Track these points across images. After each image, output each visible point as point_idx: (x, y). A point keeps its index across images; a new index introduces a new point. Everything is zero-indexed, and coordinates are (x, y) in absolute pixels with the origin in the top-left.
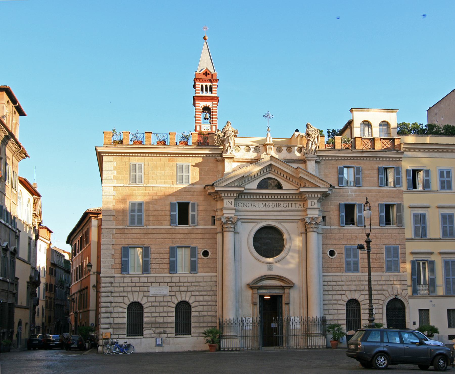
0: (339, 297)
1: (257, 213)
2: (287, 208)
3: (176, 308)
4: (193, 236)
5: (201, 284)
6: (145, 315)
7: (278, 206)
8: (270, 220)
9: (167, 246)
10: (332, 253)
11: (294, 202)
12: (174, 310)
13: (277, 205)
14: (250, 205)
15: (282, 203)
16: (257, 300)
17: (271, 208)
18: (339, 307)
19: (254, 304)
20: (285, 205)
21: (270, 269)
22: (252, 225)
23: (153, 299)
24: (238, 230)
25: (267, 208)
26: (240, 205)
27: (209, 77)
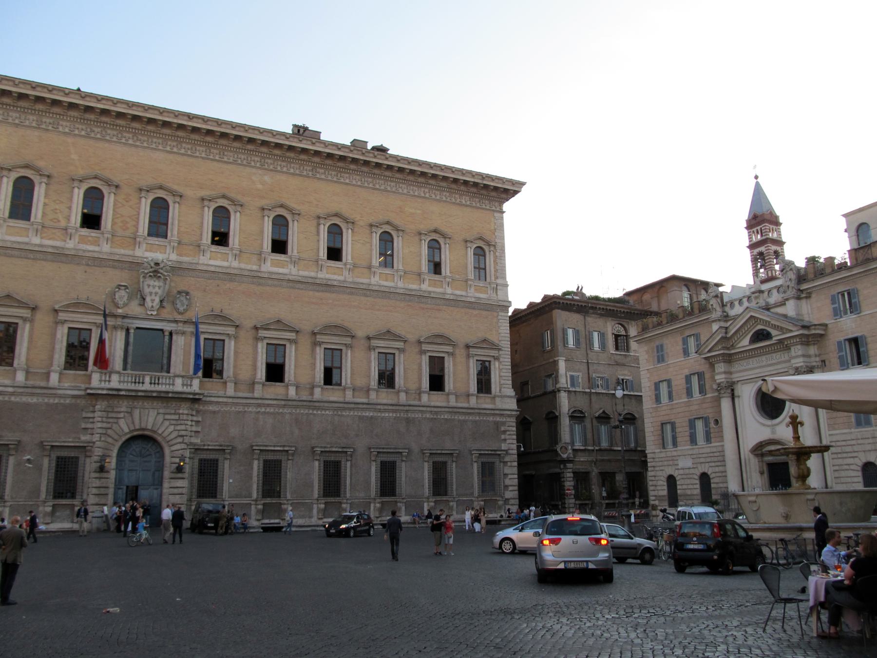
0: (851, 461)
1: (750, 372)
4: (704, 405)
5: (715, 454)
6: (678, 487)
9: (687, 419)
12: (698, 482)
15: (774, 355)
16: (765, 469)
17: (764, 363)
19: (762, 473)
21: (773, 432)
23: (681, 472)
27: (758, 220)
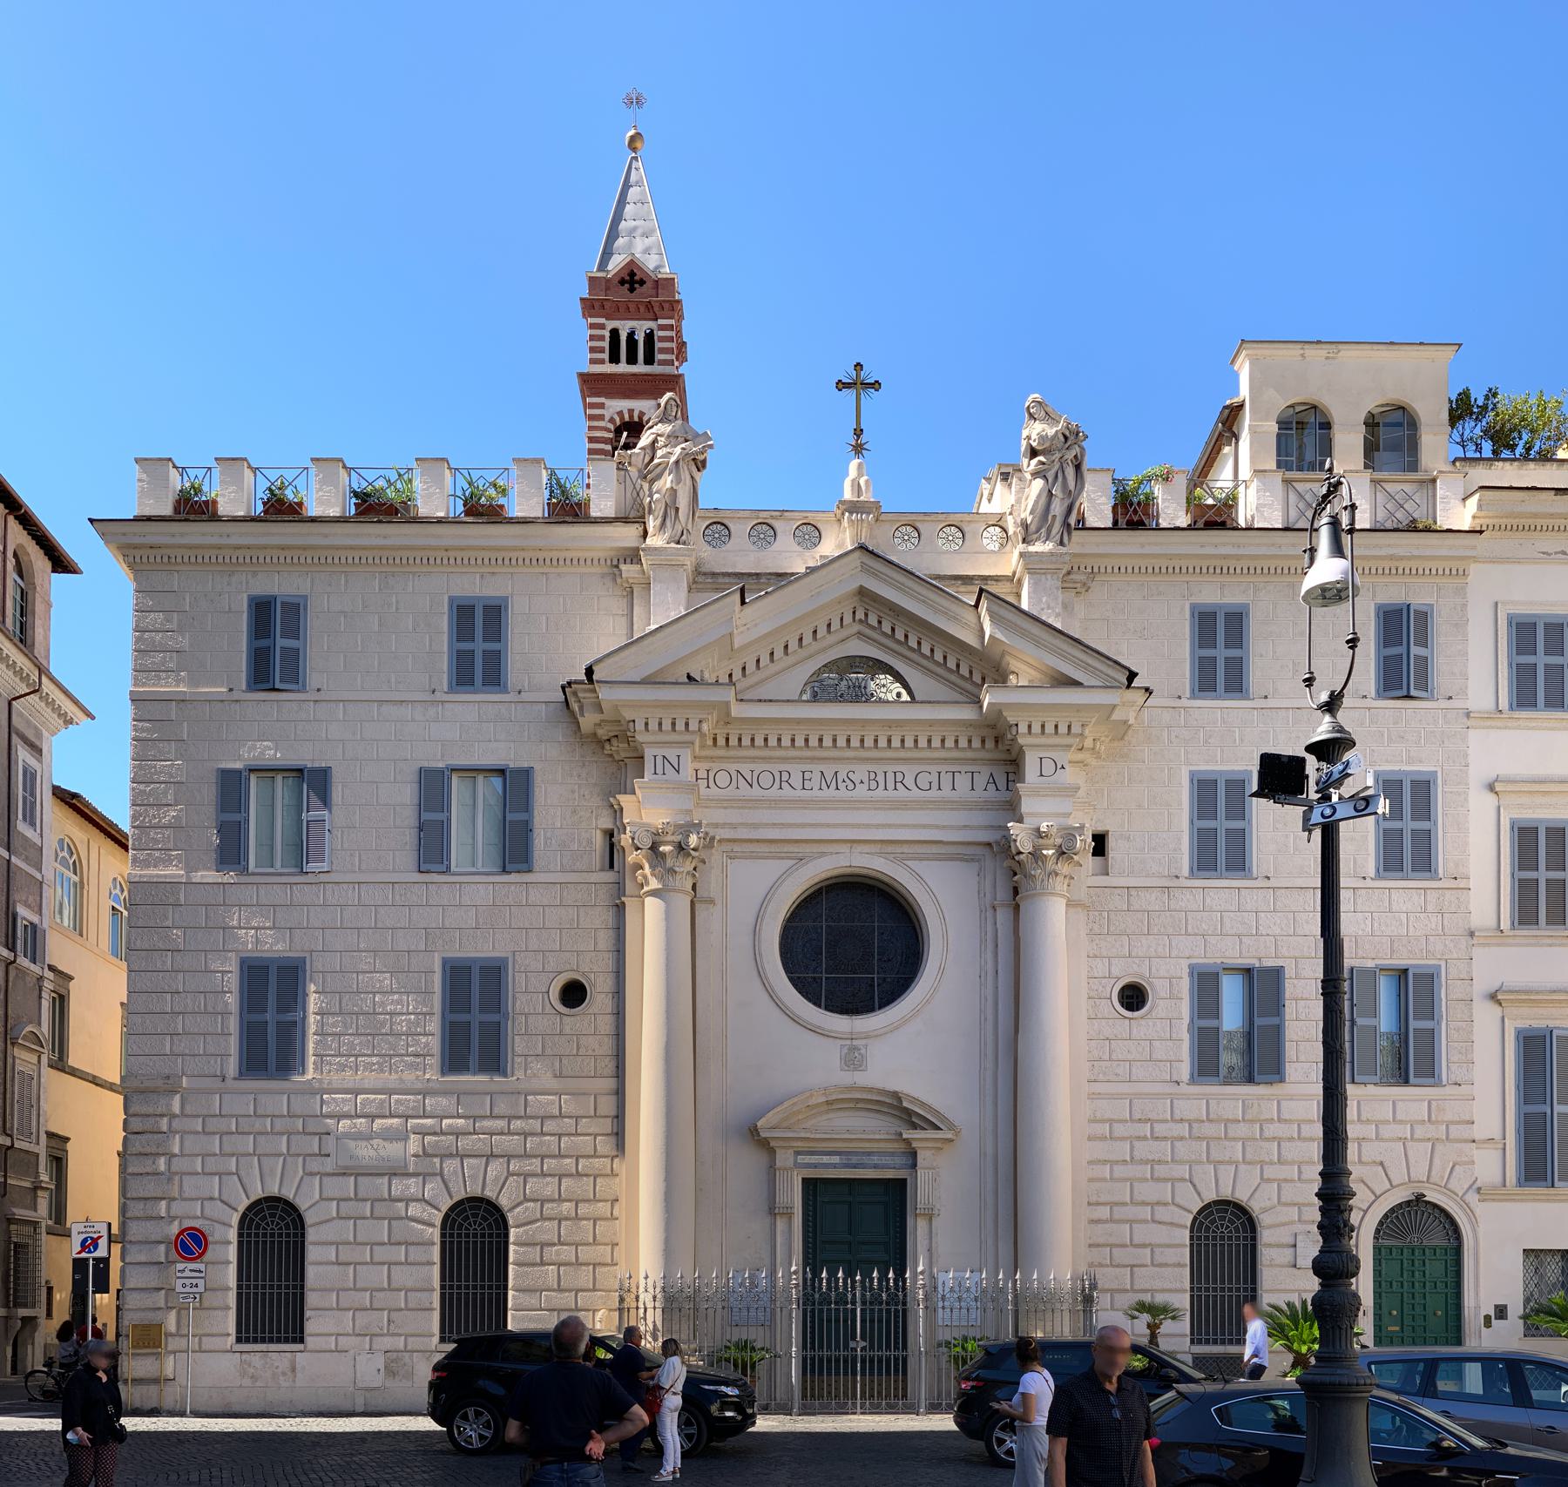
2: (934, 793)
3: (443, 1227)
7: (891, 785)
8: (860, 848)
10: (1133, 997)
11: (964, 768)
13: (890, 777)
14: (766, 780)
15: (909, 771)
18: (1159, 1235)
20: (923, 781)
21: (853, 1059)
22: (775, 868)
24: (711, 885)
25: (843, 793)
26: (723, 779)
